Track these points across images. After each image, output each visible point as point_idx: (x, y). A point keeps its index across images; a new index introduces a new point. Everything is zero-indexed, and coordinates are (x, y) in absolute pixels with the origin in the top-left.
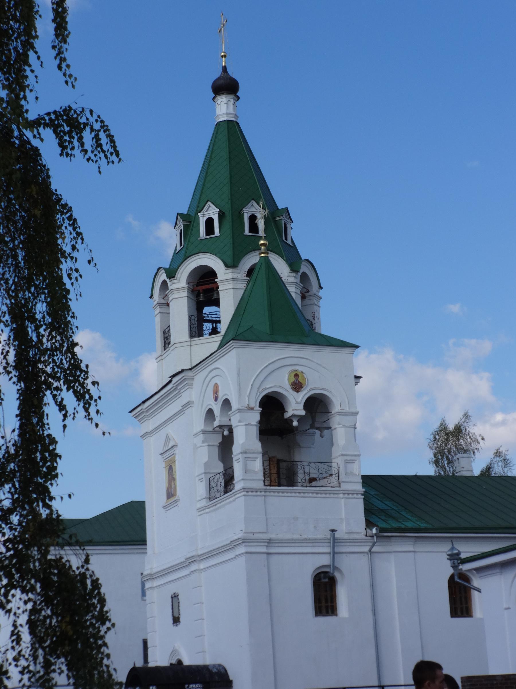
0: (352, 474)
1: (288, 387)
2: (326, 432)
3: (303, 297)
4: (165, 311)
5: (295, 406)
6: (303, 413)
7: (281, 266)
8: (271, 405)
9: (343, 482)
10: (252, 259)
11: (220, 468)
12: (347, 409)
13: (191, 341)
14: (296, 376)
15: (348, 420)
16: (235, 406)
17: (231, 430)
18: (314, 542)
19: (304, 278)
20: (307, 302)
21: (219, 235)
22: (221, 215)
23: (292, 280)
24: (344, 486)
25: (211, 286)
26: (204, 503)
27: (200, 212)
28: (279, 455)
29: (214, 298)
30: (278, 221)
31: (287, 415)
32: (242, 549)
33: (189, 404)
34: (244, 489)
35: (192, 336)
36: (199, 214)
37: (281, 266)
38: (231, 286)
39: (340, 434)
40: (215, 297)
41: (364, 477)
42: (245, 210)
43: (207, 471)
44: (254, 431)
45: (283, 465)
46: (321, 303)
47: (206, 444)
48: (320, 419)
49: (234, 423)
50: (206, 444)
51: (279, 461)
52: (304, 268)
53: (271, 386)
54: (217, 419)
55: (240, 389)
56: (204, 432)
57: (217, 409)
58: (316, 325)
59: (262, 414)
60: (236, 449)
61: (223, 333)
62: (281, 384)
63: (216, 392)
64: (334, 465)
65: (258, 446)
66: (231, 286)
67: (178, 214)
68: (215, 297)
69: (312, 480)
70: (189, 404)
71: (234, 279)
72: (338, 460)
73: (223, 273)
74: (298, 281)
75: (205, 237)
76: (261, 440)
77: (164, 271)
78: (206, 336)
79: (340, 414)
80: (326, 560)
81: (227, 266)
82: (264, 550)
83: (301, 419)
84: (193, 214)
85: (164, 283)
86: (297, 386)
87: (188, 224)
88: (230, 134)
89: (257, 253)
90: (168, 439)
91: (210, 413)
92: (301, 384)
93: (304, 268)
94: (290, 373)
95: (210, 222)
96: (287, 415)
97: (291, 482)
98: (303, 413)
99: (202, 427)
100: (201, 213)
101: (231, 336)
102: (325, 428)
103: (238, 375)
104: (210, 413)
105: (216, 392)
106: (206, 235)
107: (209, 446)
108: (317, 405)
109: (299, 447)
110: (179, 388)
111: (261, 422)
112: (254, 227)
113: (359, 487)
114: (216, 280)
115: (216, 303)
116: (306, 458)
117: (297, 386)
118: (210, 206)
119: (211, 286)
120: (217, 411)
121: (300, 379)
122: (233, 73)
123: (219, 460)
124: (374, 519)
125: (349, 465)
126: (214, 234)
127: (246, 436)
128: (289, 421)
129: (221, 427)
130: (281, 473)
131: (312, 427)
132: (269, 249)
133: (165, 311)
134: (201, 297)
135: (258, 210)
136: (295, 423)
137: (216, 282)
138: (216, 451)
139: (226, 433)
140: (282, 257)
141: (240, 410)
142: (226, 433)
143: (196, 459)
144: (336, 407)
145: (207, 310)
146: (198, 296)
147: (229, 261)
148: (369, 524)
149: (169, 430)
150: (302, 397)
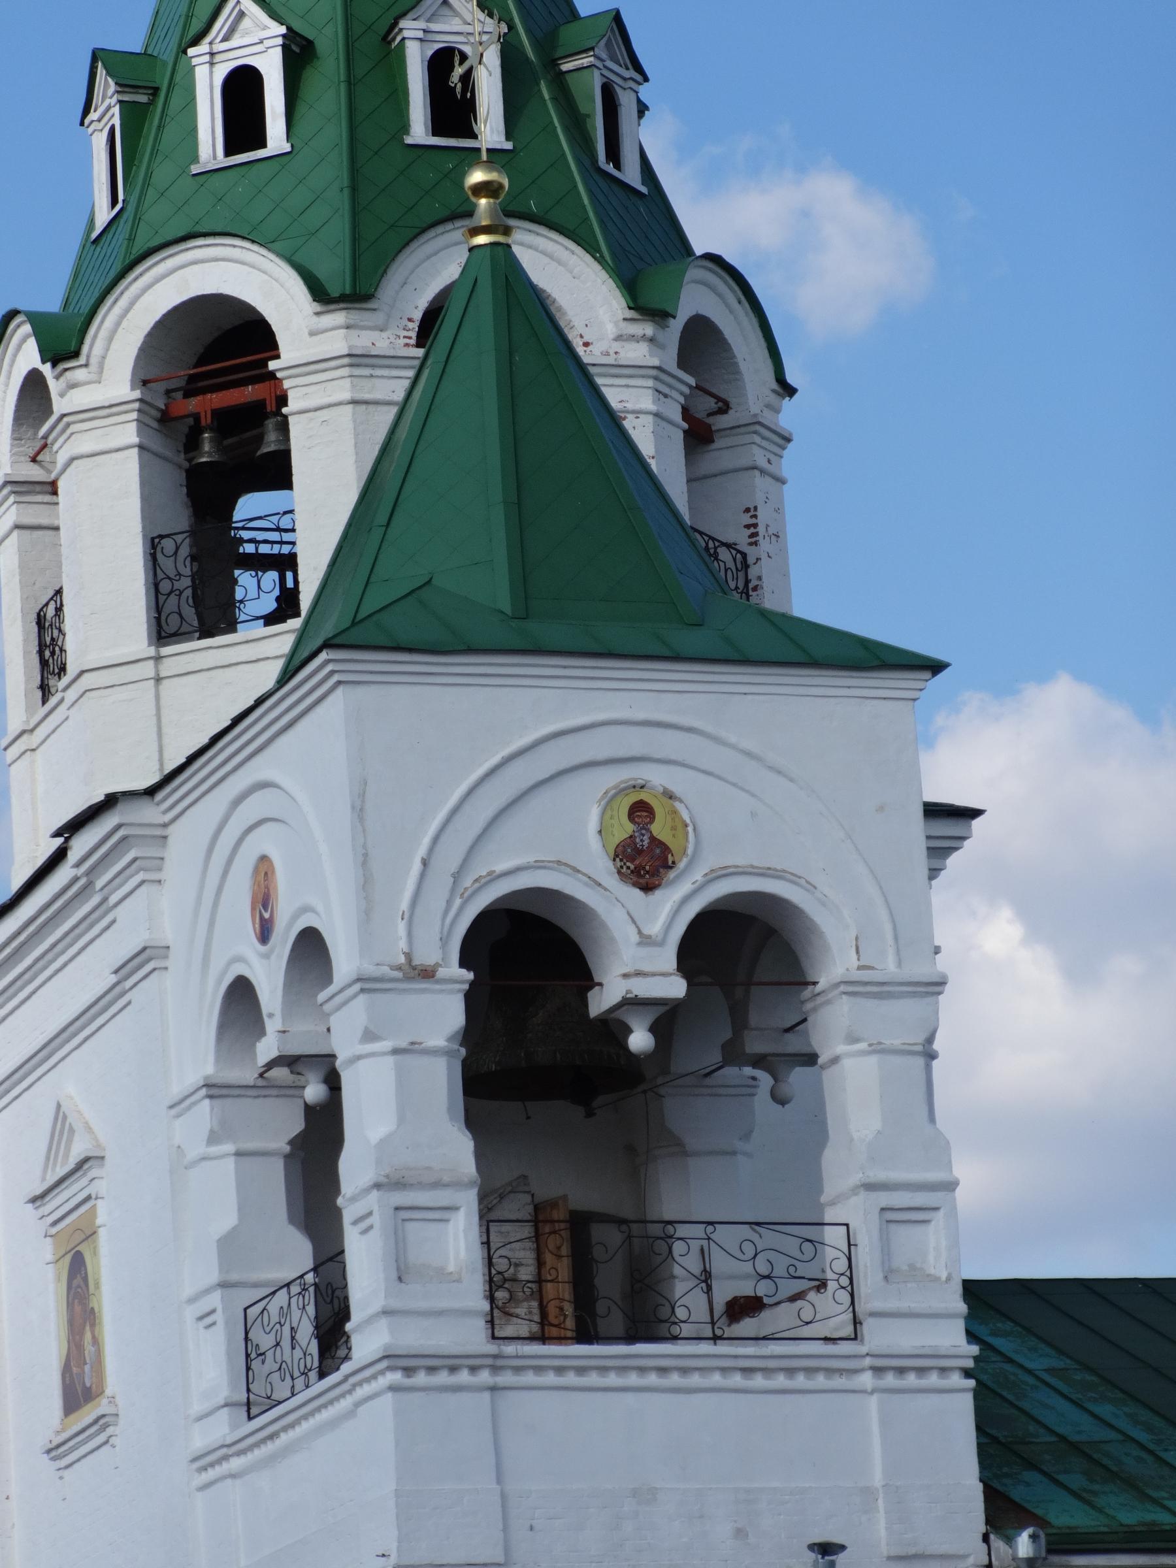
0: (918, 1275)
1: (603, 867)
2: (798, 1076)
3: (698, 436)
4: (34, 515)
5: (636, 955)
6: (676, 988)
7: (578, 288)
8: (522, 956)
9: (873, 1314)
10: (438, 266)
11: (296, 1255)
12: (889, 967)
13: (158, 659)
14: (641, 811)
15: (897, 1021)
16: (345, 961)
17: (333, 1081)
19: (700, 345)
20: (718, 457)
21: (287, 147)
22: (298, 54)
23: (638, 353)
24: (877, 1337)
25: (249, 393)
26: (223, 1428)
27: (195, 42)
28: (582, 1192)
29: (265, 449)
31: (601, 1002)
33: (142, 961)
34: (391, 1359)
35: (163, 632)
36: (191, 51)
37: (578, 288)
38: (342, 391)
39: (855, 1085)
40: (270, 444)
41: (973, 1290)
42: (410, 28)
43: (234, 1277)
44: (440, 1080)
45: (606, 1237)
46: (790, 462)
47: (229, 1148)
48: (767, 1014)
49: (344, 1044)
50: (229, 1148)
51: (580, 1224)
52: (697, 297)
53: (515, 865)
54: (272, 1026)
55: (366, 883)
56: (214, 1090)
58: (764, 570)
59: (471, 998)
60: (356, 1168)
61: (304, 613)
62: (564, 851)
63: (263, 900)
64: (834, 1237)
65: (458, 1151)
66: (342, 391)
67: (96, 56)
68: (270, 444)
69: (743, 1307)
70: (142, 961)
71: (357, 359)
72: (849, 1210)
73: (303, 332)
74: (669, 358)
75: (222, 161)
76: (472, 1122)
77: (27, 328)
78: (244, 632)
79: (855, 988)
81: (320, 293)
83: (667, 1019)
84: (166, 52)
85: (34, 386)
86: (645, 862)
87: (143, 99)
89: (454, 233)
90: (61, 1125)
91: (241, 994)
92: (666, 849)
93: (697, 297)
94: (609, 802)
95: (243, 88)
96: (601, 1002)
97: (646, 1321)
98: (676, 988)
99: (209, 1069)
100: (203, 47)
101: (327, 630)
103: (359, 812)
104: (241, 994)
105: (263, 900)
106: (229, 151)
107: (238, 1154)
108: (746, 951)
109: (679, 1148)
110: (99, 884)
111: (475, 1035)
112: (453, 110)
113: (951, 1338)
114: (272, 365)
115: (276, 473)
116: (705, 1204)
117: (645, 862)
118: (242, 14)
119: (249, 393)
120: (270, 991)
121: (659, 829)
123: (292, 1220)
124: (1027, 1489)
125: (903, 1236)
126: (262, 144)
127: (403, 1106)
128: (612, 1029)
129: (290, 1061)
130: (588, 1276)
131: (733, 1054)
132: (513, 210)
133: (34, 515)
134: (207, 447)
136: (640, 1040)
137: (272, 375)
138: (273, 1179)
139: (314, 1091)
140: (591, 248)
141: (367, 984)
142: (314, 1091)
143: (188, 1216)
144: (836, 961)
145: (251, 506)
146: (191, 444)
147: (335, 271)
148: (1002, 1512)
149: (71, 1082)
150: (670, 910)
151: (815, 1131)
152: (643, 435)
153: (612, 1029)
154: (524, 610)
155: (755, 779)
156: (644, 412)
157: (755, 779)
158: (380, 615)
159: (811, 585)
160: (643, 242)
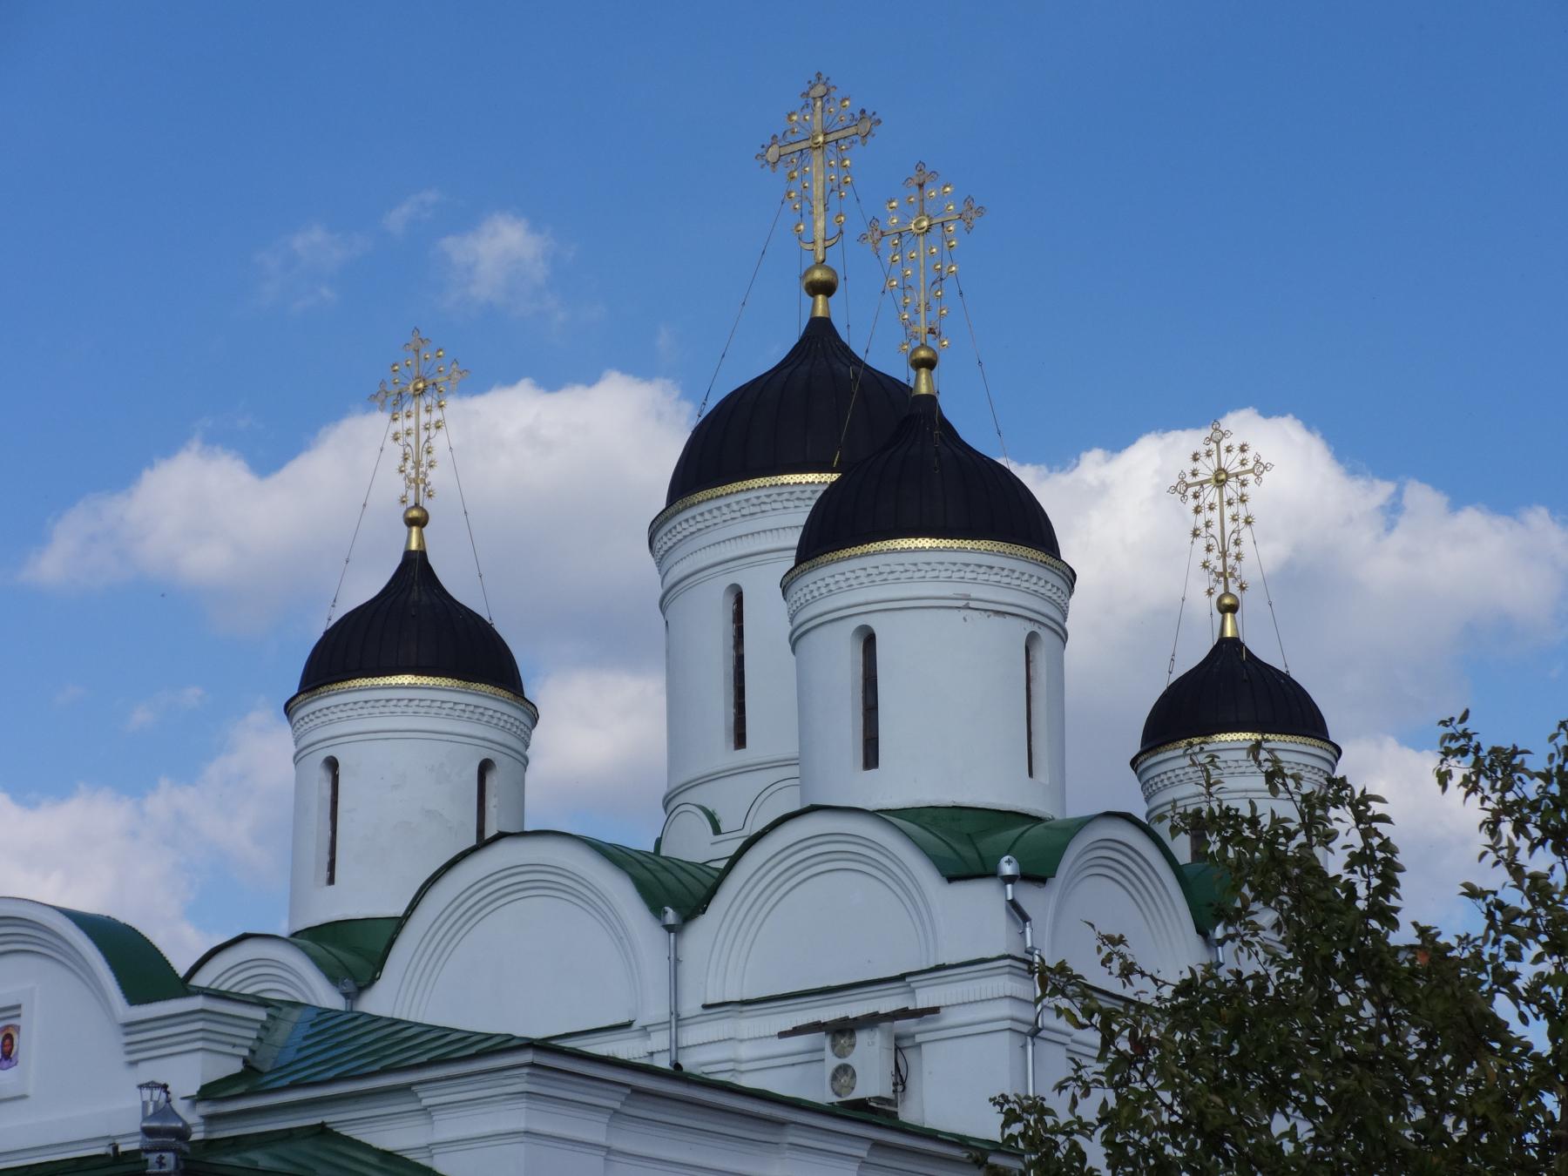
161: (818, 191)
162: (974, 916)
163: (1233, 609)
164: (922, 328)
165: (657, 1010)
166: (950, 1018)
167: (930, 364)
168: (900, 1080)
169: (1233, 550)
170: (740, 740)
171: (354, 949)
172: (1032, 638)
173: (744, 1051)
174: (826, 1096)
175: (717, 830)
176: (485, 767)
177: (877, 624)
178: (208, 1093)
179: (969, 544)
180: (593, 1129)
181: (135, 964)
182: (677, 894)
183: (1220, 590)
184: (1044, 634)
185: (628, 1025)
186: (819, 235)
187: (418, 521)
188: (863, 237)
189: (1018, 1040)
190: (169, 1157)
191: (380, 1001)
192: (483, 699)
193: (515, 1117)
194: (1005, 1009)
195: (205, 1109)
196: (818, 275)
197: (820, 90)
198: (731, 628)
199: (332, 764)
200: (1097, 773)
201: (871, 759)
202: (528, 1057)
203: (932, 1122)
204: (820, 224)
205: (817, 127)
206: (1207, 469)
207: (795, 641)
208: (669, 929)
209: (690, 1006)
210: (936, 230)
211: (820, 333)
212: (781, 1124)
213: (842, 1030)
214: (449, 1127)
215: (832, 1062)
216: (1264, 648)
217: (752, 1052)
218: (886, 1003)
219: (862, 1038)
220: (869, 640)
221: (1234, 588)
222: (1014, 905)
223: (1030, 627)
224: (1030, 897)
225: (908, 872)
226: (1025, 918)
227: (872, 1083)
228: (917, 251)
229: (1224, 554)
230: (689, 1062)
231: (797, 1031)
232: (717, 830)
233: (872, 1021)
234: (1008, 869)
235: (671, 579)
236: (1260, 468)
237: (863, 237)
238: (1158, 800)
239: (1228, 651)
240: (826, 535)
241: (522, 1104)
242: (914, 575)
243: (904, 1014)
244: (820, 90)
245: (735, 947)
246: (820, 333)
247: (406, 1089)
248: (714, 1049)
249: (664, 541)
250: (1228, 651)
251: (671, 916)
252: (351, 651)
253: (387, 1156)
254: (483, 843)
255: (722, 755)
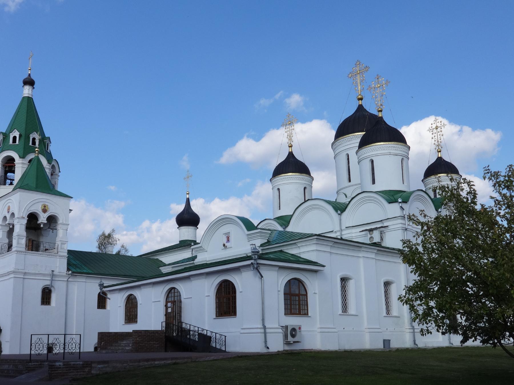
0: (63, 249)
1: (41, 211)
2: (55, 231)
3: (52, 175)
5: (43, 219)
6: (46, 222)
7: (44, 161)
8: (32, 217)
10: (31, 156)
11: (7, 241)
12: (65, 222)
14: (45, 206)
15: (65, 227)
16: (16, 216)
17: (13, 226)
18: (44, 275)
19: (53, 167)
20: (53, 177)
22: (20, 136)
23: (48, 167)
24: (59, 253)
25: (12, 165)
28: (33, 238)
30: (45, 142)
31: (38, 222)
32: (12, 276)
34: (16, 251)
37: (44, 161)
38: (21, 166)
39: (60, 232)
40: (13, 169)
42: (31, 135)
44: (24, 227)
45: (35, 242)
46: (59, 178)
48: (53, 225)
49: (15, 223)
51: (33, 241)
52: (54, 163)
53: (33, 210)
54: (8, 221)
57: (8, 216)
58: (56, 187)
59: (28, 221)
60: (15, 234)
61: (15, 185)
62: (37, 209)
63: (9, 209)
64: (56, 245)
65: (25, 234)
66: (21, 166)
68: (13, 169)
69: (46, 250)
71: (22, 163)
72: (58, 243)
74: (50, 168)
76: (26, 231)
78: (7, 185)
79: (61, 224)
80: (48, 283)
81: (20, 157)
82: (22, 276)
86: (45, 211)
88: (28, 104)
89: (34, 154)
91: (5, 218)
94: (42, 205)
95: (15, 138)
96: (38, 222)
98: (46, 222)
101: (18, 187)
102: (55, 229)
103: (20, 203)
104: (5, 218)
105: (9, 209)
108: (52, 220)
109: (42, 235)
111: (27, 224)
112: (34, 143)
113: (66, 254)
115: (13, 172)
116: (45, 240)
117: (45, 211)
119: (12, 165)
121: (46, 208)
122: (33, 77)
127: (20, 229)
128: (40, 224)
129: (9, 224)
130: (33, 246)
131: (49, 228)
132: (39, 153)
135: (37, 137)
136: (42, 226)
138: (6, 234)
139: (11, 227)
141: (18, 218)
142: (11, 227)
144: (60, 221)
145: (9, 174)
146: (6, 168)
147: (22, 156)
148: (68, 269)
150: (46, 215)
151: (56, 235)
152: (48, 173)
153: (40, 224)
154: (37, 188)
155: (55, 205)
156: (48, 171)
157: (55, 205)
158: (23, 186)
159: (60, 188)
160: (49, 158)
161: (359, 81)
162: (394, 209)
163: (440, 151)
164: (379, 104)
165: (337, 228)
166: (390, 227)
167: (381, 111)
168: (382, 239)
169: (440, 141)
170: (350, 181)
171: (284, 221)
172: (402, 159)
173: (353, 235)
174: (369, 242)
175: (346, 197)
176: (305, 188)
177: (373, 158)
178: (262, 245)
179: (390, 143)
180: (328, 249)
181: (249, 225)
182: (340, 208)
183: (437, 148)
184: (404, 158)
185: (332, 231)
186: (359, 90)
187: (291, 146)
188: (368, 89)
189: (403, 231)
190: (256, 256)
191: (289, 229)
192: (304, 176)
193: (314, 247)
194: (401, 225)
195: (262, 248)
196: (360, 97)
197: (358, 63)
198: (347, 161)
199: (279, 189)
200: (415, 182)
201: (374, 182)
202: (316, 237)
203: (388, 246)
204: (360, 88)
205: (358, 70)
206: (434, 126)
207: (359, 163)
208: (339, 214)
209: (343, 227)
210: (381, 87)
211: (360, 107)
212: (361, 247)
213: (371, 230)
214: (302, 250)
215: (369, 236)
216: (446, 158)
217: (355, 235)
218: (378, 225)
219: (375, 232)
220: (372, 162)
221: (440, 148)
222: (401, 207)
223: (402, 157)
224: (404, 205)
225: (380, 201)
226: (403, 209)
227: (377, 239)
228: (378, 91)
229: (438, 142)
230: (344, 237)
231: (363, 231)
232: (346, 197)
233: (376, 229)
234: (400, 200)
235: (336, 153)
236: (429, 130)
237: (368, 89)
238: (427, 187)
239: (439, 159)
240: (364, 143)
241: (315, 245)
242: (380, 149)
243: (382, 227)
244: (358, 63)
245: (350, 217)
246: (360, 107)
247: (295, 243)
248: (347, 235)
249: (334, 147)
250: (439, 159)
251: (339, 212)
252: (281, 169)
253: (292, 255)
254: (305, 201)
255: (347, 184)
